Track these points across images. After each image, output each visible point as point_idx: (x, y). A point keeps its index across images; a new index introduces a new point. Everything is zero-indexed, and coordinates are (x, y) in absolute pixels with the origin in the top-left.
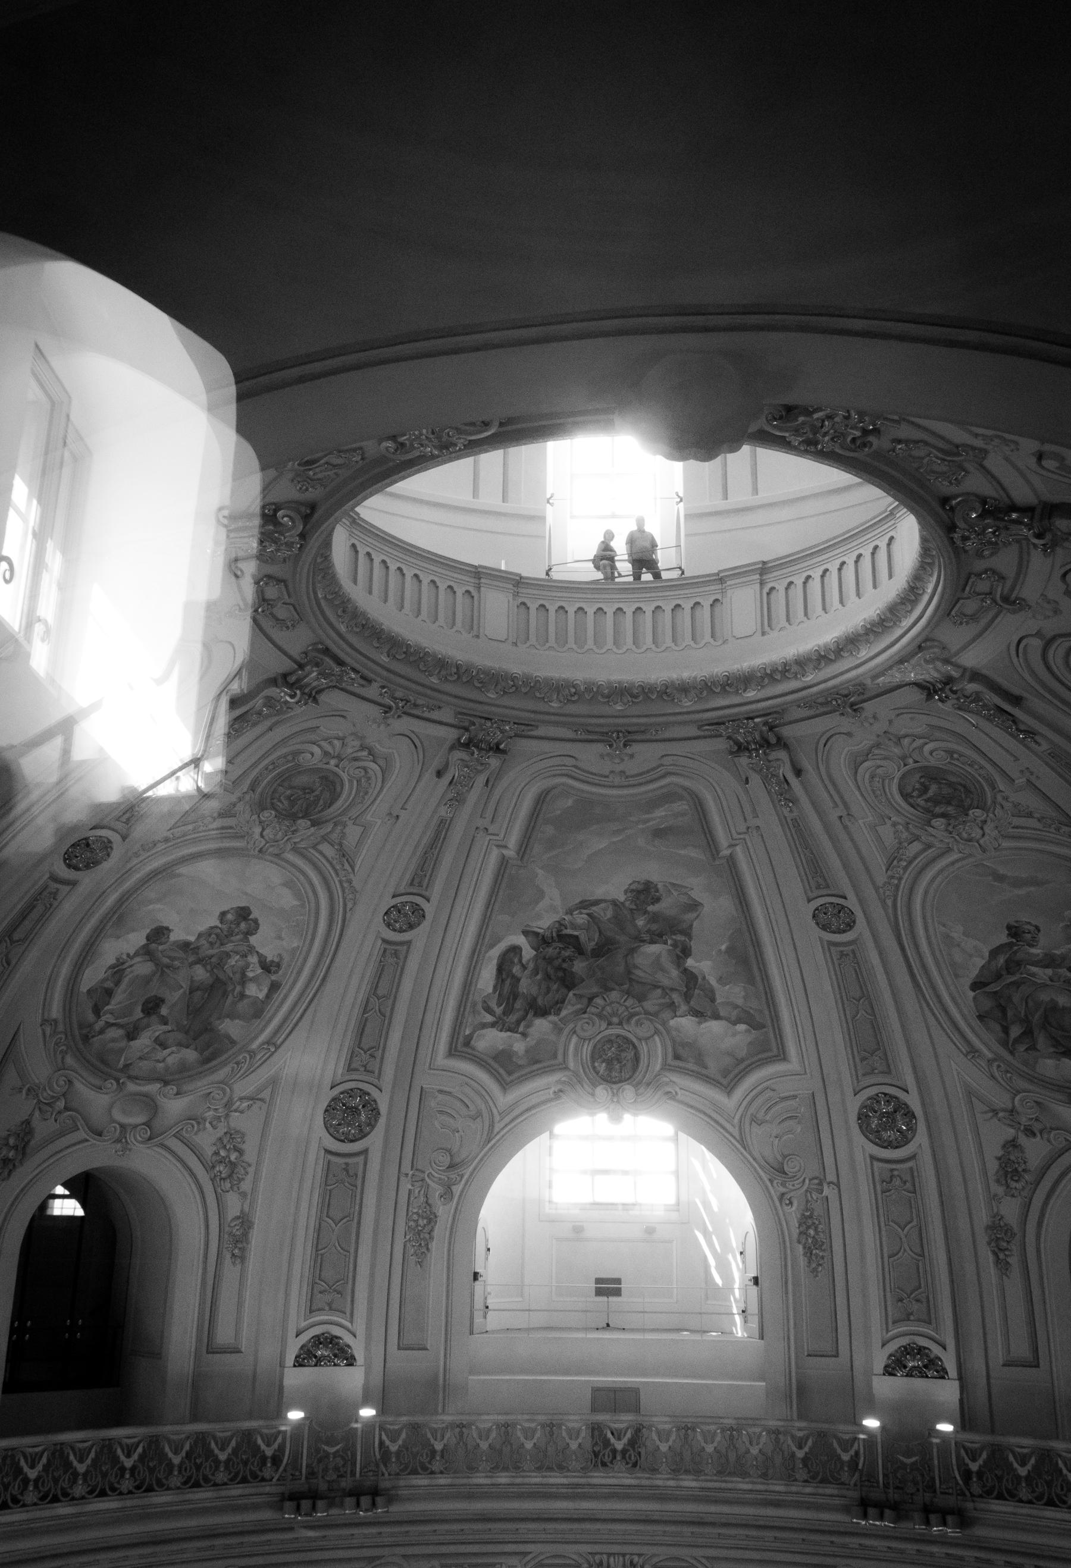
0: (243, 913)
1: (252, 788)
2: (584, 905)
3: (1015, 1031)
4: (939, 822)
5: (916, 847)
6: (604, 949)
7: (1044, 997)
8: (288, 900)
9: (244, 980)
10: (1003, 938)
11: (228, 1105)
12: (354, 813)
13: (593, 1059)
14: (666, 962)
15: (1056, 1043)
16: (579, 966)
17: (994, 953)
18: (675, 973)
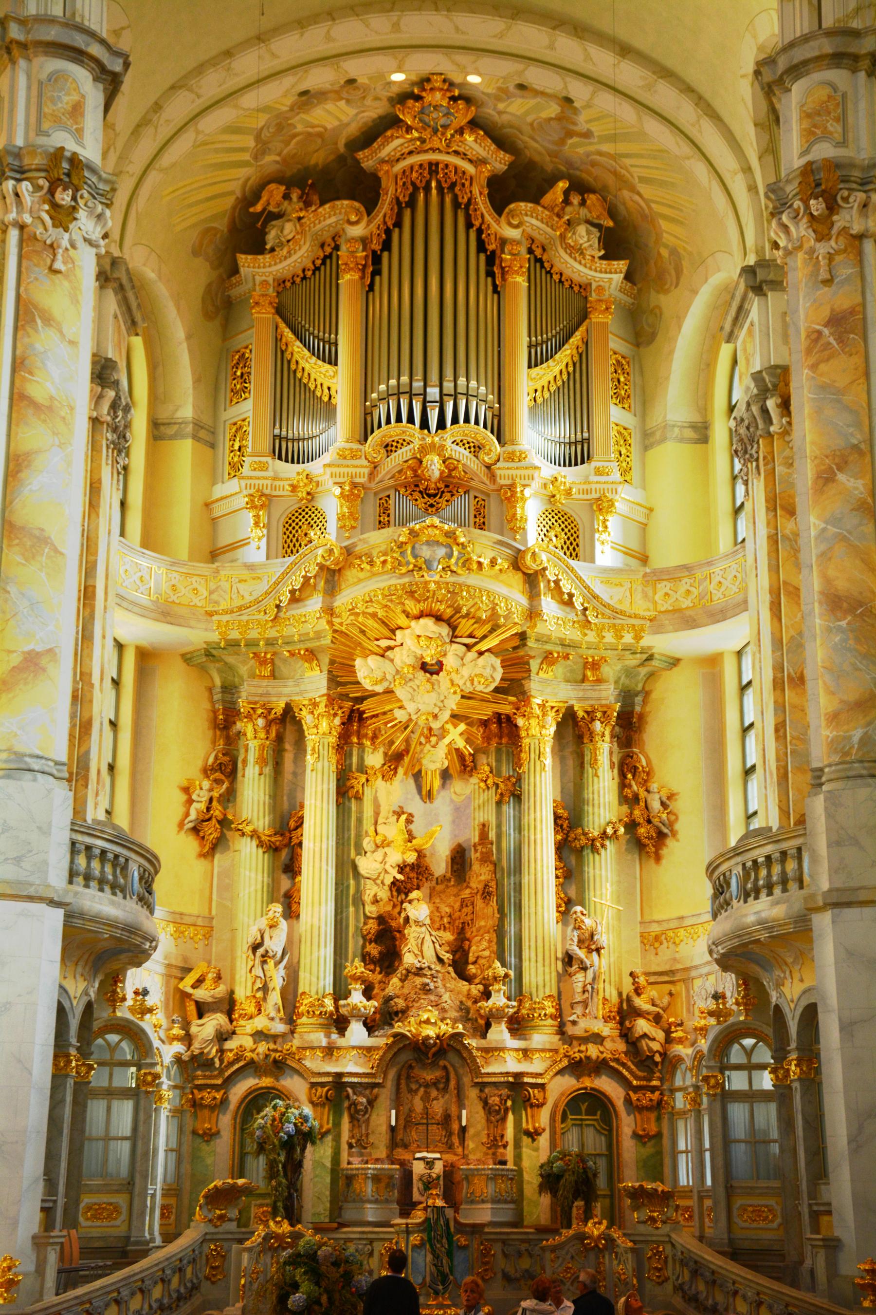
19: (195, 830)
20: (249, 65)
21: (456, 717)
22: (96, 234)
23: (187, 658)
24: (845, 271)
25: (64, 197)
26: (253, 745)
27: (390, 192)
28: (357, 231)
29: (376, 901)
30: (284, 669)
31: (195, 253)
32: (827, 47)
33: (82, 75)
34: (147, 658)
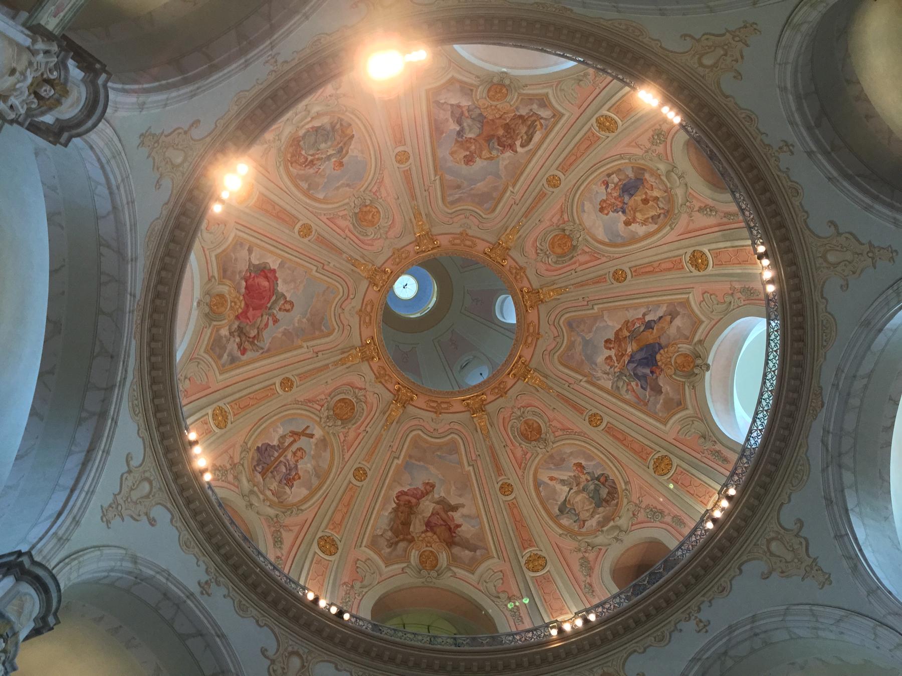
0: (602, 210)
1: (573, 257)
2: (491, 159)
3: (338, 126)
4: (368, 202)
5: (374, 190)
6: (489, 139)
7: (329, 143)
8: (588, 206)
9: (616, 185)
10: (345, 160)
11: (647, 152)
12: (552, 228)
13: (507, 94)
14: (467, 128)
15: (324, 129)
16: (501, 132)
17: (347, 152)
18: (465, 124)
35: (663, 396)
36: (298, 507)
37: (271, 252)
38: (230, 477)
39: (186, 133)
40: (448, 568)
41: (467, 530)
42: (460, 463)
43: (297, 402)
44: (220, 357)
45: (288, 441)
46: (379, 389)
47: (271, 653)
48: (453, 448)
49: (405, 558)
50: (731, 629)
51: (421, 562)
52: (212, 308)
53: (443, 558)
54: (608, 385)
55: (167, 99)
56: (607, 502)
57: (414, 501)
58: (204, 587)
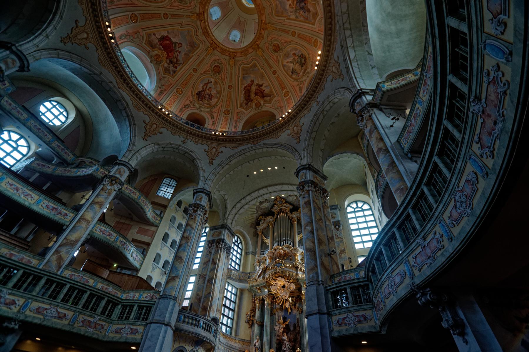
19: (248, 322)
20: (248, 198)
21: (290, 297)
22: (202, 215)
23: (248, 290)
24: (306, 195)
25: (196, 209)
26: (258, 305)
27: (276, 213)
28: (271, 220)
29: (278, 336)
30: (262, 290)
31: (251, 227)
32: (301, 167)
33: (204, 195)
34: (242, 291)
35: (311, 13)
36: (216, 105)
37: (162, 30)
38: (192, 106)
39: (77, 27)
40: (264, 105)
41: (267, 91)
42: (259, 69)
43: (201, 74)
44: (170, 73)
45: (205, 87)
46: (224, 56)
47: (207, 150)
48: (255, 66)
49: (251, 106)
50: (323, 103)
51: (256, 106)
52: (156, 61)
53: (262, 102)
54: (293, 17)
55: (54, 26)
56: (304, 64)
57: (249, 88)
58: (184, 142)
